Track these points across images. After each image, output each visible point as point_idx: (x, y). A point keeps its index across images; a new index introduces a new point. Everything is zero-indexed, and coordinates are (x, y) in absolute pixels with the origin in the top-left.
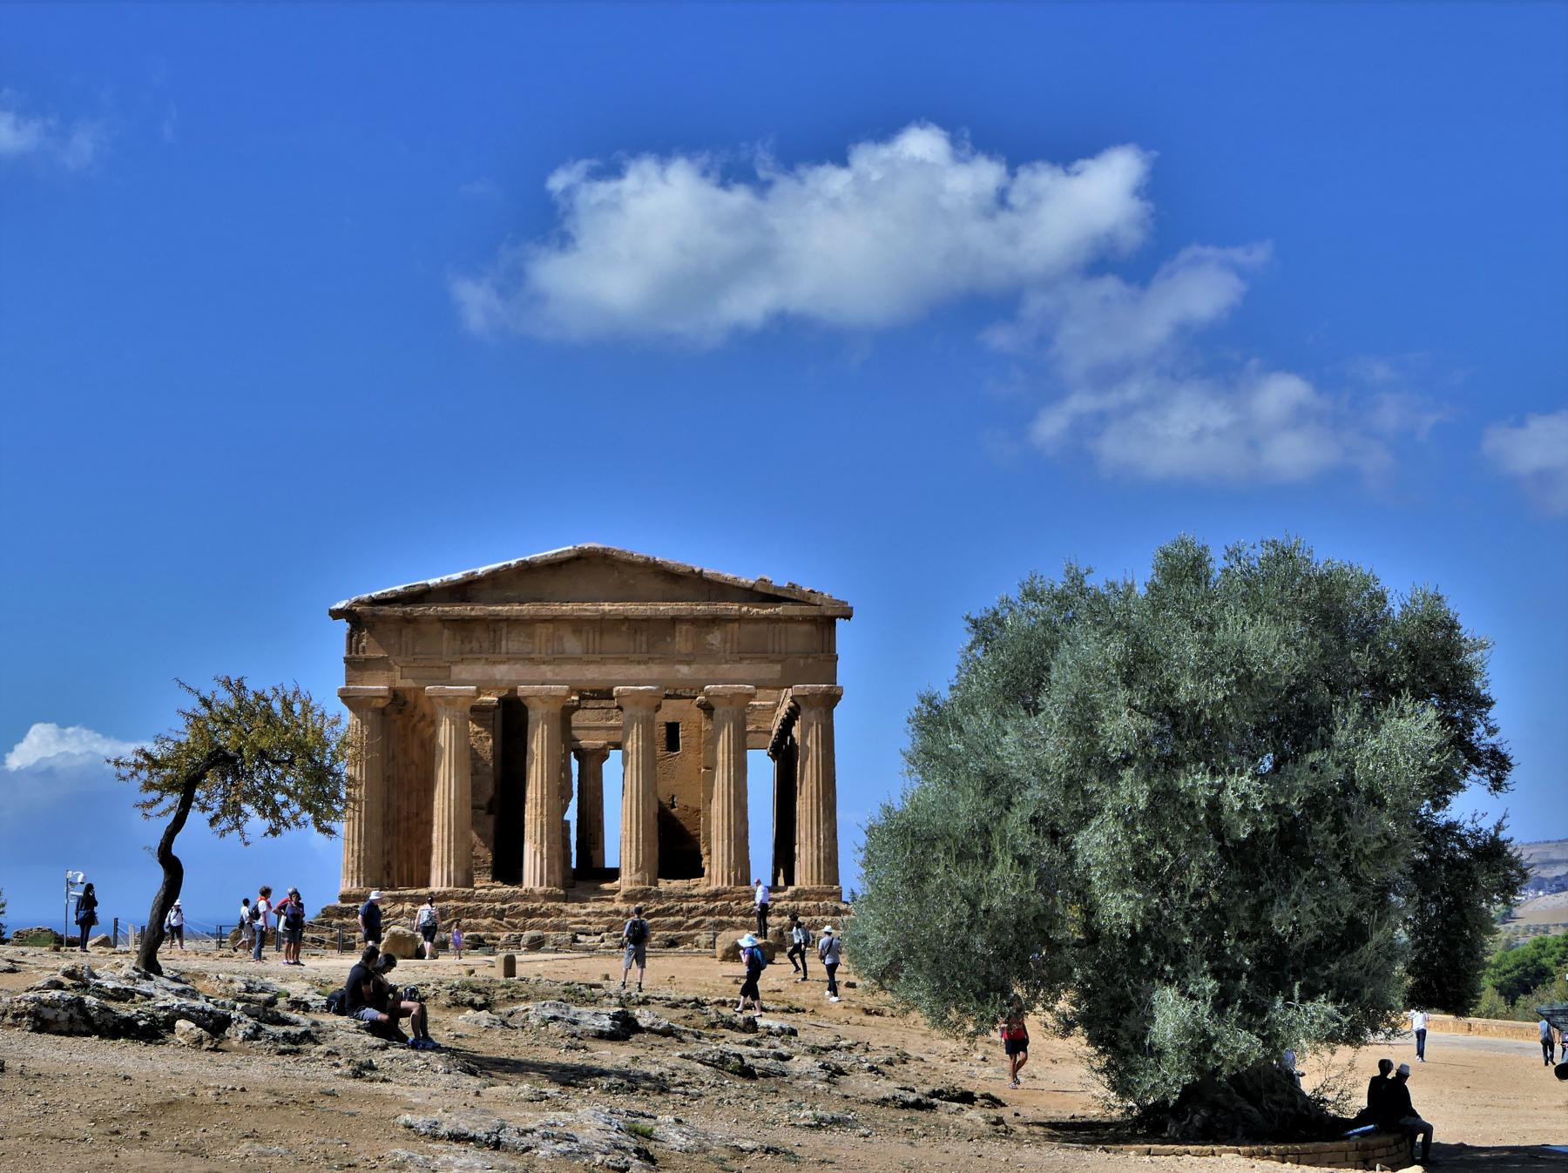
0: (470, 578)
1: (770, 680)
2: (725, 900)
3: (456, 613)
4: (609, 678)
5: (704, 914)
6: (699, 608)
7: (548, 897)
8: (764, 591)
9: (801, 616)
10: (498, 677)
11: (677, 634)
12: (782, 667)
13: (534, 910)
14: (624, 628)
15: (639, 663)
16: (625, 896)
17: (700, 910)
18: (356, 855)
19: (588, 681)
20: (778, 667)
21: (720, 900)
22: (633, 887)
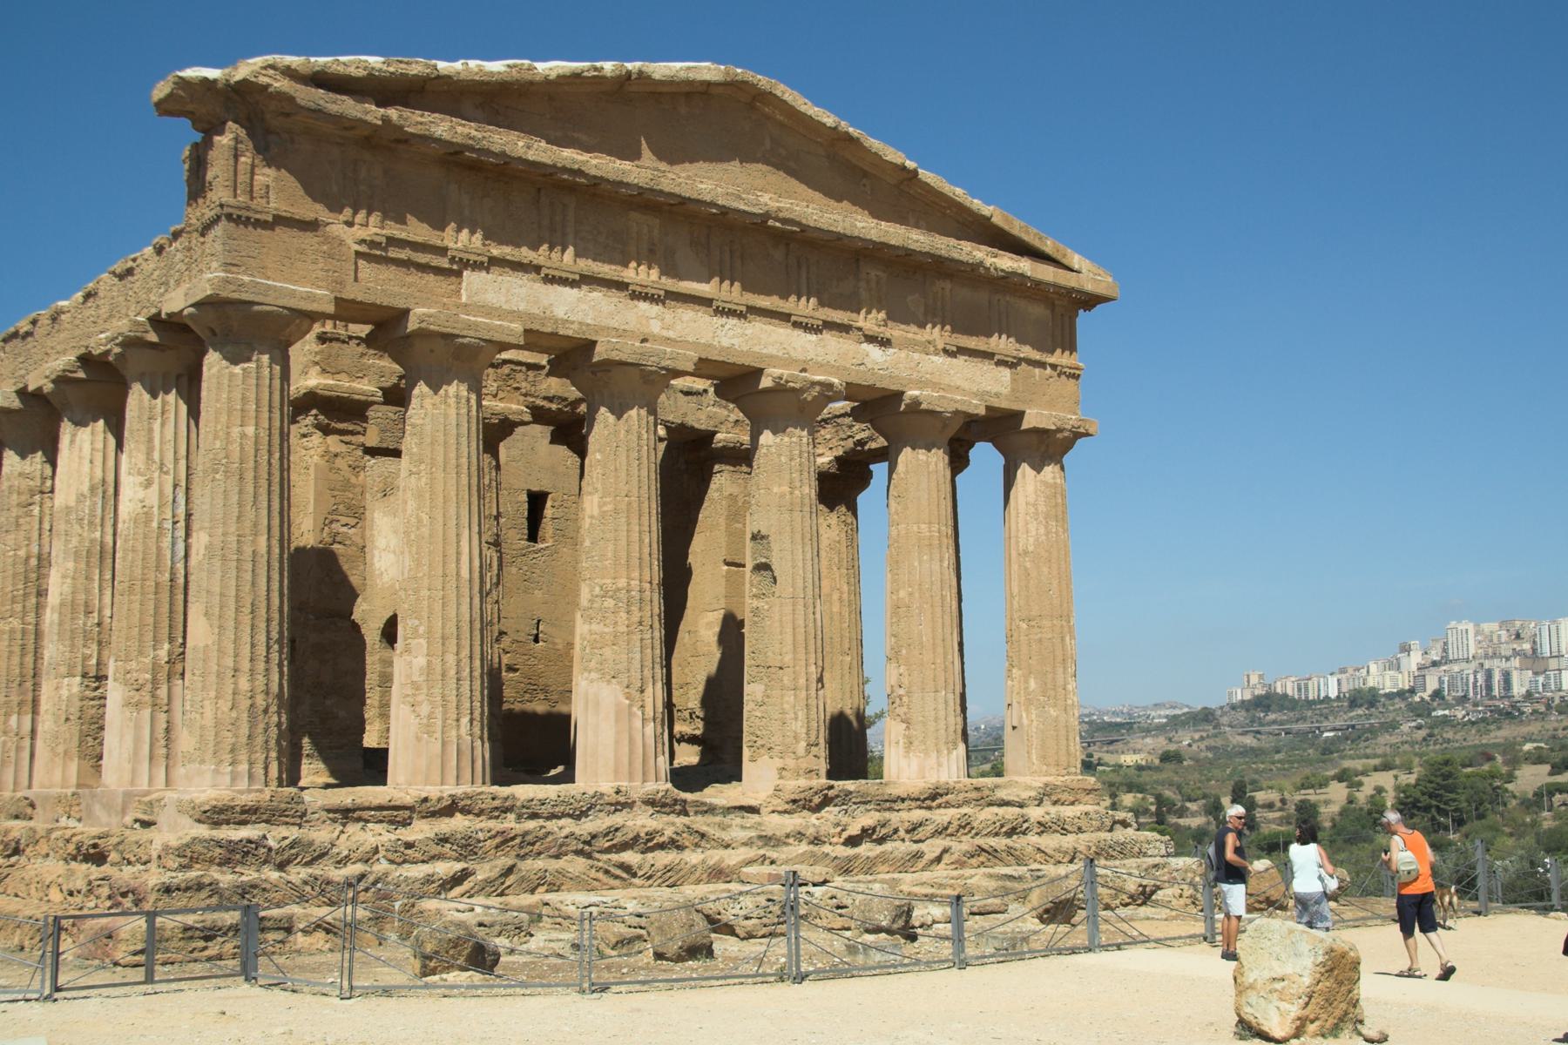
0: (528, 76)
1: (997, 395)
2: (948, 805)
3: (496, 148)
4: (756, 349)
5: (938, 833)
6: (915, 237)
7: (656, 804)
8: (1006, 228)
9: (1055, 285)
10: (560, 312)
11: (862, 284)
12: (1014, 380)
13: (651, 835)
14: (778, 254)
15: (807, 328)
16: (794, 801)
17: (930, 828)
18: (245, 704)
19: (723, 349)
20: (1006, 373)
21: (939, 806)
22: (803, 782)
